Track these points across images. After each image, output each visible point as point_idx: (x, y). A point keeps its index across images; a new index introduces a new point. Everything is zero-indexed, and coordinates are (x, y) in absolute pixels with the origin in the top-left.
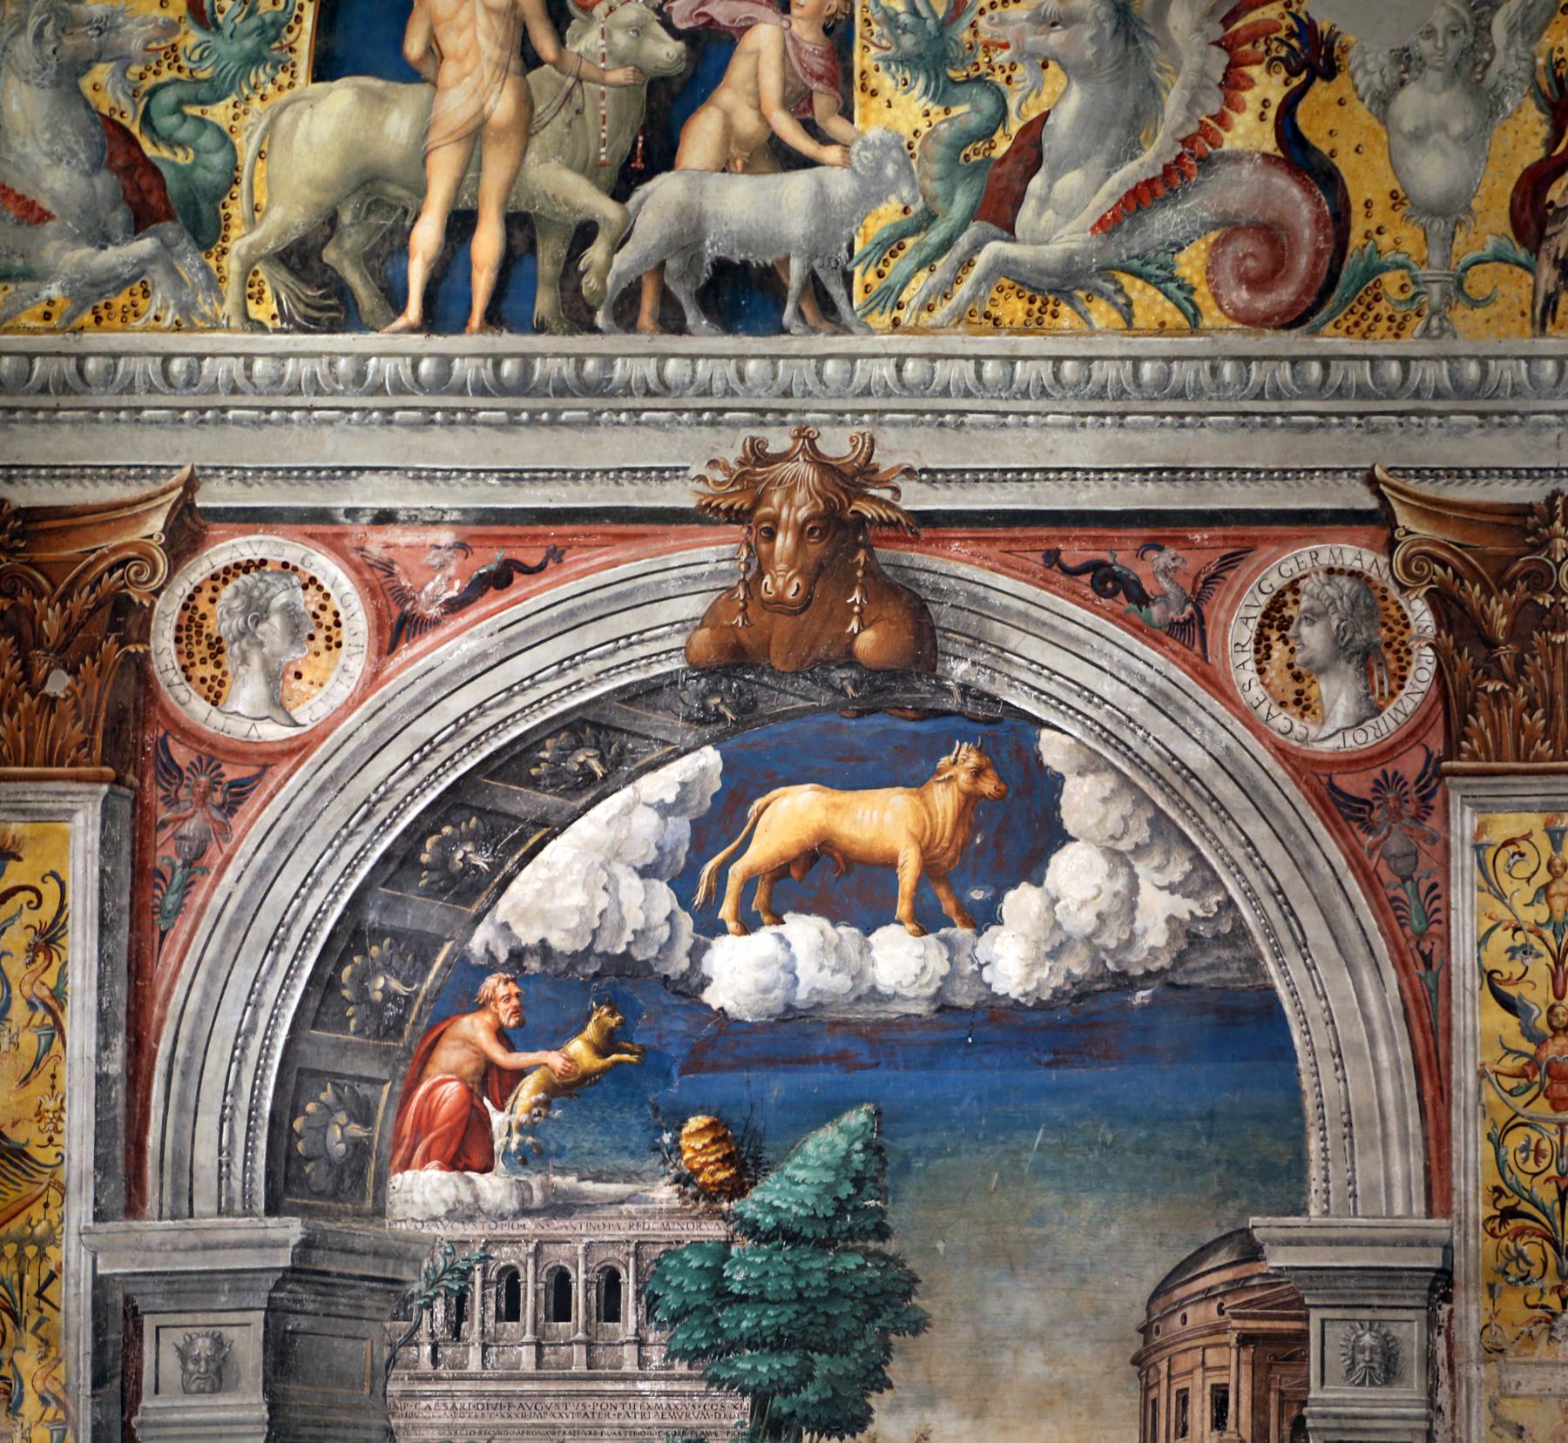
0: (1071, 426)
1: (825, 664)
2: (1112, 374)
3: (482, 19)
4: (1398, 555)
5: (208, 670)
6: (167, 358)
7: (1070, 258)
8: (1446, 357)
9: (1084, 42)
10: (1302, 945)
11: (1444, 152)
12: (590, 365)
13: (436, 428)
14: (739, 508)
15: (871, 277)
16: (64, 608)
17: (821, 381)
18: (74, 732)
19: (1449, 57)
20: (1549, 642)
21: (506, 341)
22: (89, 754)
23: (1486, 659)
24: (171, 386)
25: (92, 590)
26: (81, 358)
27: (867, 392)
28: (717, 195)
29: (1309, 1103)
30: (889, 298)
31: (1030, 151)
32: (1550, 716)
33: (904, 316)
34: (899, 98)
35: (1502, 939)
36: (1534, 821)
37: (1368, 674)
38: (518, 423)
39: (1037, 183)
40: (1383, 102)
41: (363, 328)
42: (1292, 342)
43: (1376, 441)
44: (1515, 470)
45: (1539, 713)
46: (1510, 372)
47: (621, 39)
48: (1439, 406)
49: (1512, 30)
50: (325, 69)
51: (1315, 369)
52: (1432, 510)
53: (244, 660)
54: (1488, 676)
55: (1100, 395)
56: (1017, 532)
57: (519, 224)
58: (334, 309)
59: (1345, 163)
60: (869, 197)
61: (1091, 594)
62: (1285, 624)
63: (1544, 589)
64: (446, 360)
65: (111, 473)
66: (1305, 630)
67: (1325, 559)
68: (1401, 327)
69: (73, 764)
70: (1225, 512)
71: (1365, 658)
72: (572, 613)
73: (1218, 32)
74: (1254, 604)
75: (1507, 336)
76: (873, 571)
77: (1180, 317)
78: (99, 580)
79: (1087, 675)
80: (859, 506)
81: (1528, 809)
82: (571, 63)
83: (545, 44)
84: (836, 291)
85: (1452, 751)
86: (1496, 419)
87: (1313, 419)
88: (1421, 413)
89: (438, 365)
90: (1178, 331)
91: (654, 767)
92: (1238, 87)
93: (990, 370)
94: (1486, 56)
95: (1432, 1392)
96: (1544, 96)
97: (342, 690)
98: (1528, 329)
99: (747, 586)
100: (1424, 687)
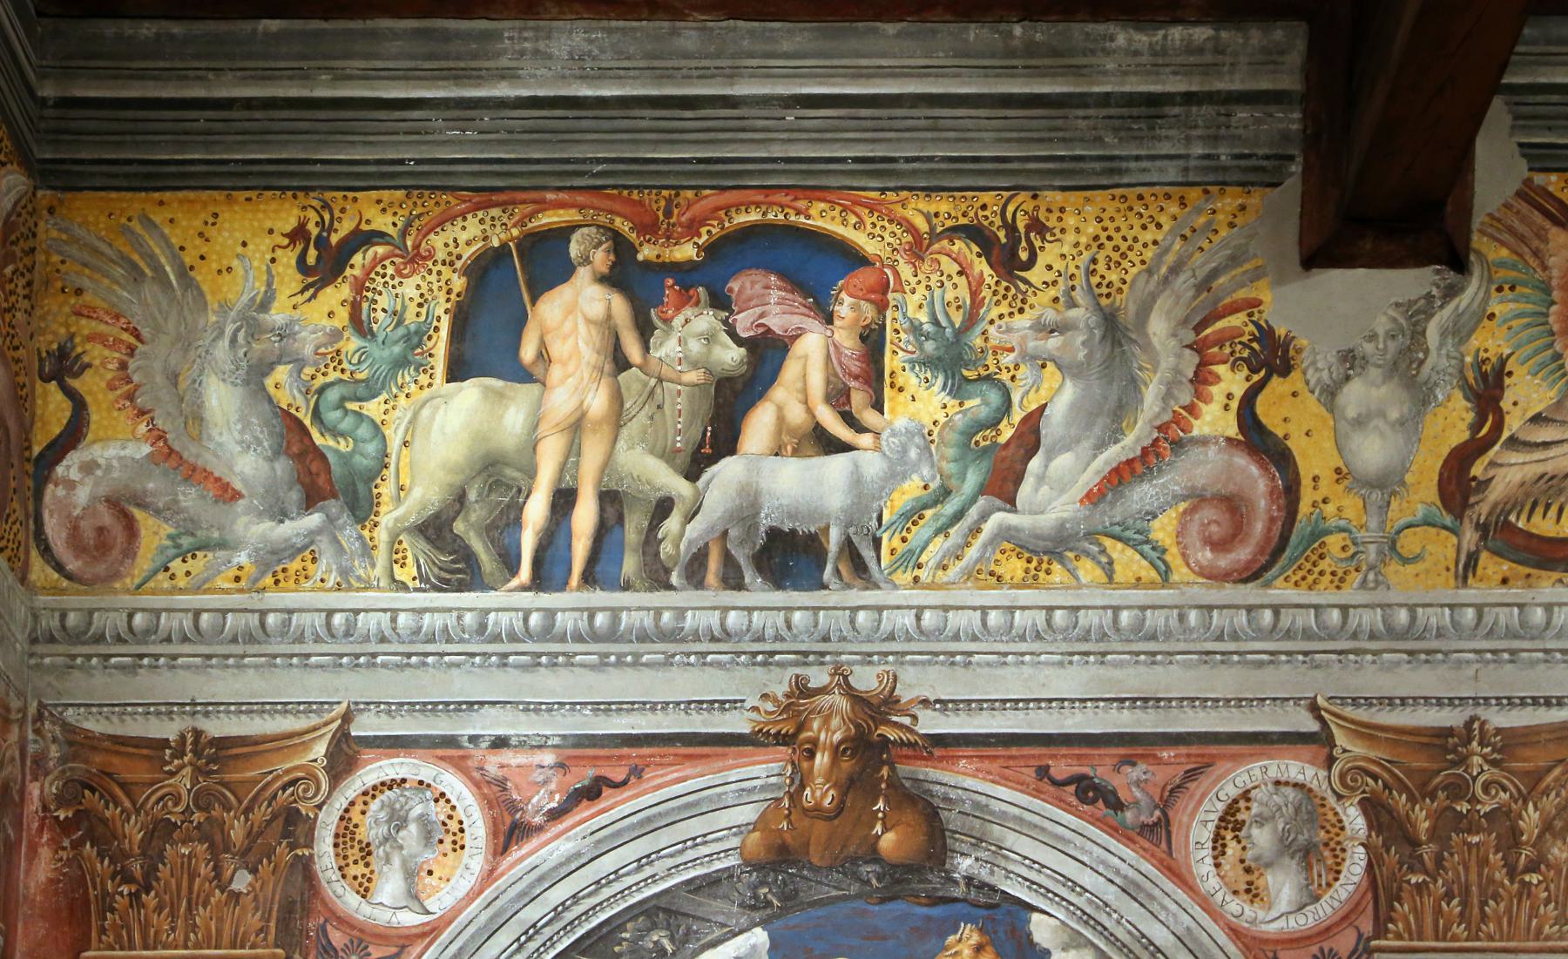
0: (1061, 664)
1: (854, 860)
2: (1096, 621)
3: (582, 328)
4: (1336, 769)
5: (359, 870)
6: (330, 613)
7: (1062, 525)
8: (1381, 606)
9: (1077, 346)
11: (1382, 435)
12: (666, 617)
13: (542, 669)
14: (786, 733)
15: (896, 542)
16: (247, 820)
17: (854, 628)
18: (254, 920)
19: (1389, 357)
20: (1465, 842)
21: (598, 597)
22: (265, 939)
23: (1411, 856)
24: (333, 636)
25: (269, 805)
26: (263, 613)
27: (891, 637)
28: (771, 475)
30: (911, 559)
31: (1030, 437)
32: (1465, 903)
33: (923, 574)
34: (922, 393)
37: (1309, 868)
38: (607, 664)
39: (1035, 464)
40: (1330, 395)
41: (485, 587)
42: (1250, 593)
43: (1318, 674)
44: (1438, 699)
45: (1455, 901)
47: (695, 347)
49: (1444, 334)
50: (458, 371)
51: (1267, 616)
52: (1366, 732)
53: (388, 861)
54: (1412, 870)
55: (1085, 638)
56: (1014, 751)
57: (610, 500)
58: (461, 572)
60: (896, 474)
61: (1073, 800)
62: (1238, 827)
63: (1462, 798)
64: (550, 614)
65: (285, 708)
66: (1255, 832)
67: (1273, 773)
68: (1342, 580)
69: (253, 947)
70: (1189, 734)
71: (1307, 855)
72: (649, 820)
73: (1190, 337)
74: (1212, 810)
75: (1434, 587)
76: (894, 783)
77: (1153, 574)
78: (275, 796)
79: (1070, 869)
80: (883, 730)
82: (654, 366)
83: (633, 351)
84: (868, 554)
85: (1380, 932)
86: (1423, 657)
87: (1265, 657)
88: (1356, 652)
89: (545, 617)
90: (1152, 585)
91: (714, 944)
92: (1206, 382)
93: (994, 618)
94: (1421, 355)
96: (1471, 388)
97: (464, 884)
98: (1452, 581)
99: (791, 796)
100: (1356, 879)
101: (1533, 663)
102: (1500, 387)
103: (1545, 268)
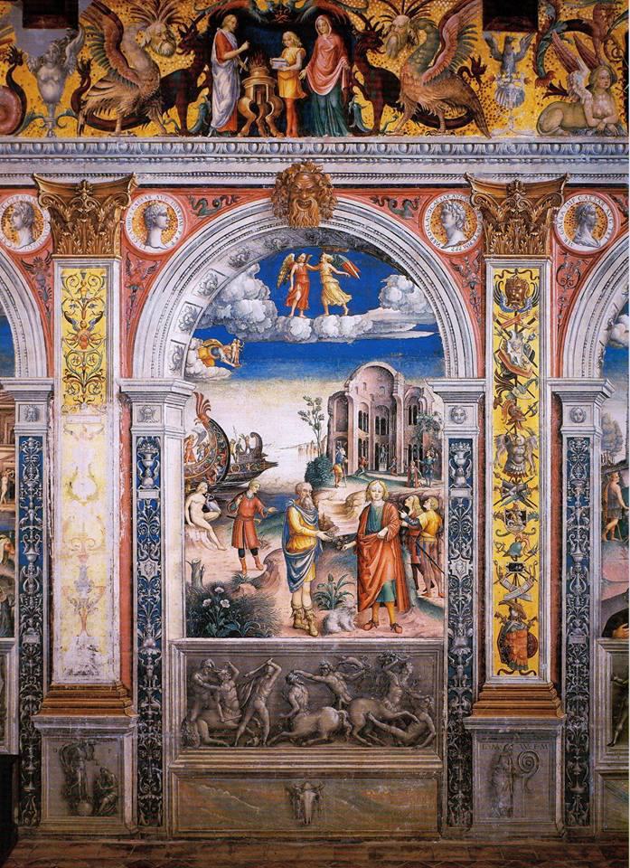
10: (14, 304)
29: (16, 348)
32: (82, 242)
35: (68, 303)
36: (77, 271)
40: (35, 71)
42: (11, 138)
46: (70, 147)
48: (52, 156)
49: (71, 51)
51: (17, 146)
52: (48, 184)
54: (65, 231)
59: (25, 89)
62: (9, 216)
66: (14, 218)
67: (20, 199)
81: (75, 267)
95: (48, 423)
101: (102, 162)
102: (89, 69)
103: (102, 29)
